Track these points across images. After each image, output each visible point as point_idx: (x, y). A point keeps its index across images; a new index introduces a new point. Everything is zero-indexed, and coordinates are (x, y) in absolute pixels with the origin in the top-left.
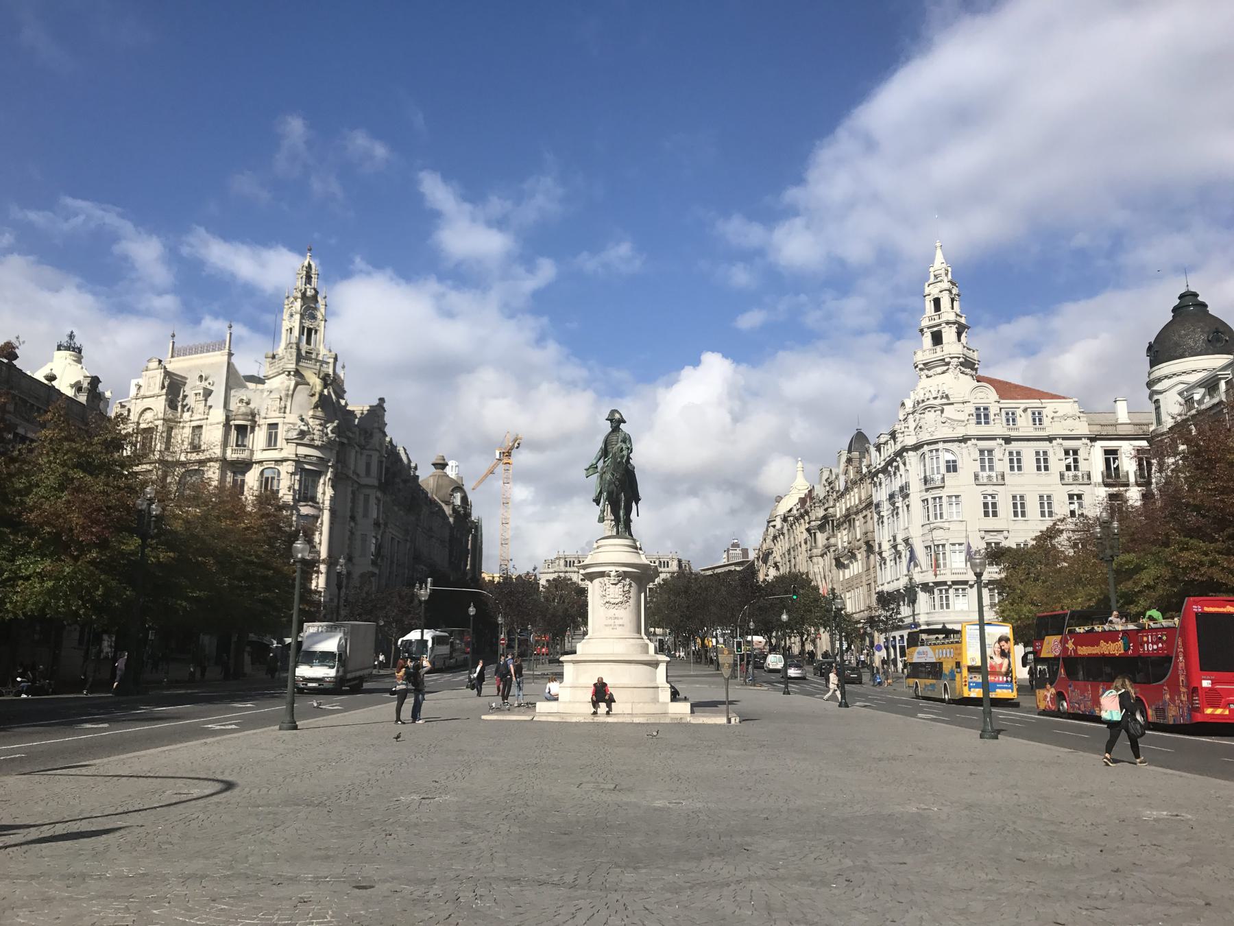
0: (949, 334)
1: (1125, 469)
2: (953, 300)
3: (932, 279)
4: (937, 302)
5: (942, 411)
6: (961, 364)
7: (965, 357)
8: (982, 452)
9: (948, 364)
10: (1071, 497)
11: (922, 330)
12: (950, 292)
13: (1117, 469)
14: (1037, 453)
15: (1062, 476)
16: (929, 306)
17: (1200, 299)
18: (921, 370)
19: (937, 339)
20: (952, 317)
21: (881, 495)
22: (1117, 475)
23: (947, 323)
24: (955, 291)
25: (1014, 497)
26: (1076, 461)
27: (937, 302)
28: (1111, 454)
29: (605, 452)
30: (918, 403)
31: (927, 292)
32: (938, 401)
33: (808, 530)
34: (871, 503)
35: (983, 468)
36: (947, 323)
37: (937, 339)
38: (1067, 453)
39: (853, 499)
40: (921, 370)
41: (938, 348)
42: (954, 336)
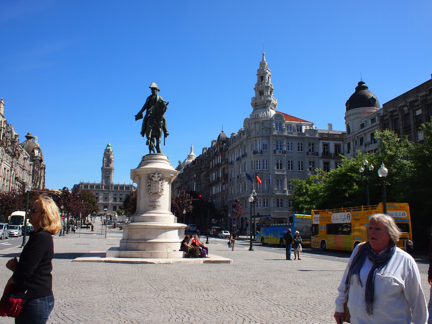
1: (331, 152)
8: (277, 143)
10: (310, 163)
13: (327, 152)
14: (299, 144)
15: (307, 154)
21: (232, 158)
22: (328, 155)
25: (289, 162)
26: (313, 148)
28: (326, 146)
29: (146, 107)
33: (196, 174)
34: (228, 162)
35: (277, 149)
38: (310, 144)
39: (219, 160)
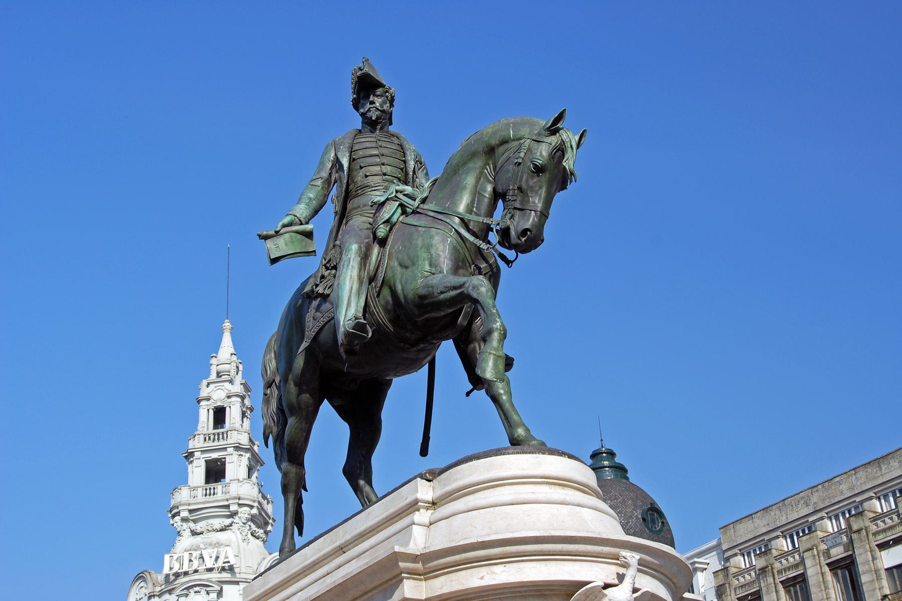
0: (237, 466)
2: (244, 415)
3: (213, 376)
4: (219, 415)
5: (220, 594)
6: (253, 519)
7: (261, 508)
9: (234, 514)
11: (190, 455)
12: (243, 398)
16: (205, 417)
17: (618, 460)
18: (185, 520)
19: (215, 472)
20: (244, 440)
23: (238, 448)
24: (247, 402)
27: (219, 415)
30: (177, 575)
31: (204, 392)
32: (215, 576)
36: (238, 448)
37: (215, 472)
40: (185, 520)
41: (219, 487)
42: (243, 472)
